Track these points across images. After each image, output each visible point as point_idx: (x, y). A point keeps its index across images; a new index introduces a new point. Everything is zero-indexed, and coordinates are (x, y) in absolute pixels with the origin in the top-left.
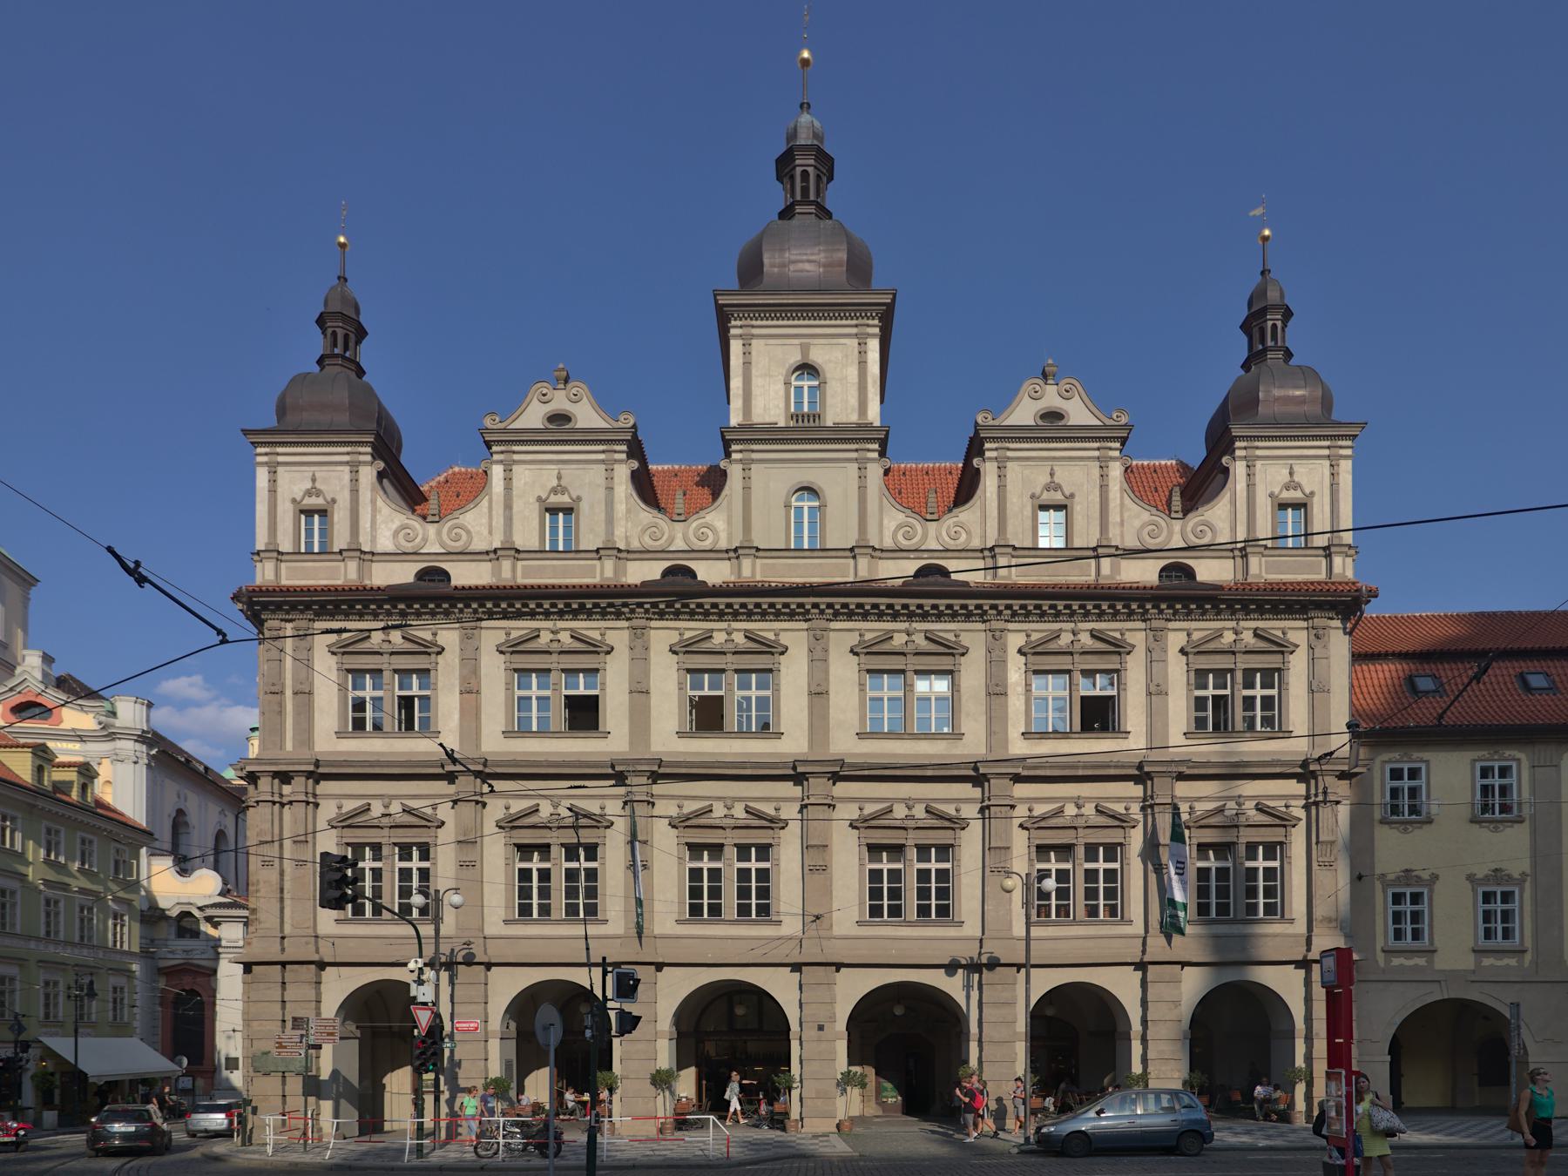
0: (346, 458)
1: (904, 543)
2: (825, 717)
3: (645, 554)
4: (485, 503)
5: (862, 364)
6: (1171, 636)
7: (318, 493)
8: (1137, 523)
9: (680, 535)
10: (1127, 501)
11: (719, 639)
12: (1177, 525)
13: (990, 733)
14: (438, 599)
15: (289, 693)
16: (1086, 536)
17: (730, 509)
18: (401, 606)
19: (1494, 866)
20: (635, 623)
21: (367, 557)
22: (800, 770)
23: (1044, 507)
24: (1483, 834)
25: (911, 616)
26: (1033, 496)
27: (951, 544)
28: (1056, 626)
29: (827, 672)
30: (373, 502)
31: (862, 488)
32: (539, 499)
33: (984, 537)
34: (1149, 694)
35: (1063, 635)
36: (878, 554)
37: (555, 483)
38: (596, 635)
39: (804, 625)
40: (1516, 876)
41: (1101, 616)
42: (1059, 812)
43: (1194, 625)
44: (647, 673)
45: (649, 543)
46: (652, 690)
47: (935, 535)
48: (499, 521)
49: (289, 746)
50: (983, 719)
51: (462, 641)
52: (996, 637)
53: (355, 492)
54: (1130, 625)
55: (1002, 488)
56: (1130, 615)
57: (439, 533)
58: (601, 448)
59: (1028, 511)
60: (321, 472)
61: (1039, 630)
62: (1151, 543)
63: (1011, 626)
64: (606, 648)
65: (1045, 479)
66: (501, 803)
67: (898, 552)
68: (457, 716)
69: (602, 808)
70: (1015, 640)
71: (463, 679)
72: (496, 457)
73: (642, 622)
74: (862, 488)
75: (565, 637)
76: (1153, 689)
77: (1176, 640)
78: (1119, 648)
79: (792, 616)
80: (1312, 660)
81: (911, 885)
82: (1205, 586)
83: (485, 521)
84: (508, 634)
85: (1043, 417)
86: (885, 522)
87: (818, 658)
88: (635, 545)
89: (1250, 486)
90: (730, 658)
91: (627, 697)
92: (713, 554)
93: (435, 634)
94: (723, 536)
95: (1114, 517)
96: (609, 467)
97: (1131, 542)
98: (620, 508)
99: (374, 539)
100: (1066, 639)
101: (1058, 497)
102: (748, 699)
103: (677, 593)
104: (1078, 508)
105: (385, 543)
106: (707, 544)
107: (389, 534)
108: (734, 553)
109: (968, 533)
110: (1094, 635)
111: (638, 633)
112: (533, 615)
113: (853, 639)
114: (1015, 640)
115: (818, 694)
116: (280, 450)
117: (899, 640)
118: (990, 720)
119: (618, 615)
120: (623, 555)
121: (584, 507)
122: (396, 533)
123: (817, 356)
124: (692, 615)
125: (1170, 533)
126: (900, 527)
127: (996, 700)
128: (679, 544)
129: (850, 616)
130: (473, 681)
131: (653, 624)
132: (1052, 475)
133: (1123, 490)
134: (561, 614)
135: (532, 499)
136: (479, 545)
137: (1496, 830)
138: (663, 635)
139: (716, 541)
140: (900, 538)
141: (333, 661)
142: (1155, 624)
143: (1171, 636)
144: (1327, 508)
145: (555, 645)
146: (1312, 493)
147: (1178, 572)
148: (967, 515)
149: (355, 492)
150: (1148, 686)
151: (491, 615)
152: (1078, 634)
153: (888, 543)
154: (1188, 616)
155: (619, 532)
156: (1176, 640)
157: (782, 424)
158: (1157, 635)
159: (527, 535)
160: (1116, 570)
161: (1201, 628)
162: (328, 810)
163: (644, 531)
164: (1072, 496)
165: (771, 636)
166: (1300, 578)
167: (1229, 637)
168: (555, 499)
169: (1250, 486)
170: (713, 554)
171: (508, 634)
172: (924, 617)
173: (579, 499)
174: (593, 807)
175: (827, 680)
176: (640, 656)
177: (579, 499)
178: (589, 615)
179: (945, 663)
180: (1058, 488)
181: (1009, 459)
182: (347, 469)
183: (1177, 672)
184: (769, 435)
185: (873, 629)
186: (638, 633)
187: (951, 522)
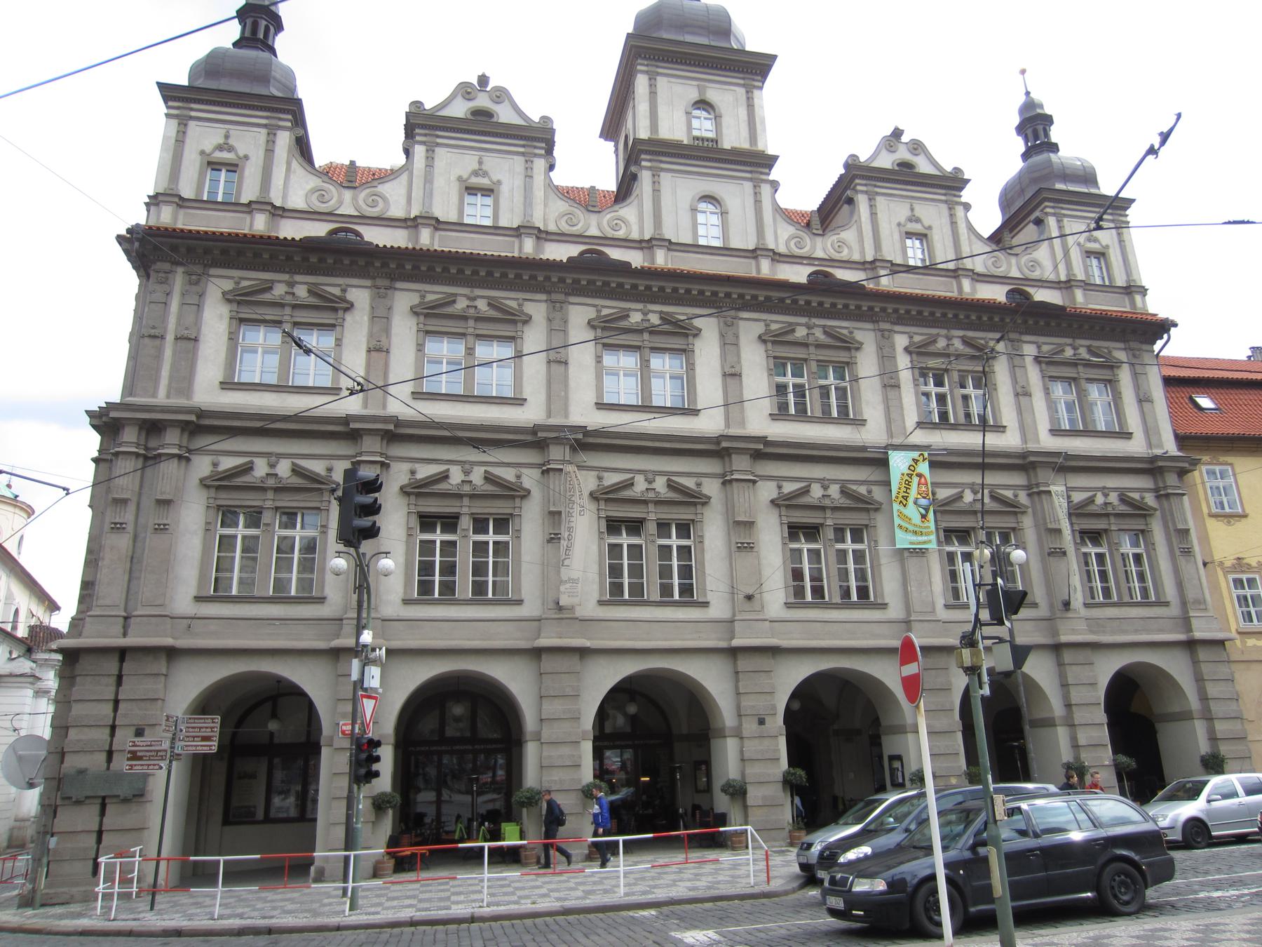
0: (264, 121)
1: (797, 252)
3: (561, 237)
7: (231, 149)
11: (636, 318)
12: (1013, 260)
13: (889, 420)
15: (170, 337)
17: (641, 206)
20: (555, 297)
23: (909, 235)
26: (899, 224)
27: (837, 256)
28: (934, 331)
29: (739, 356)
30: (289, 164)
32: (460, 179)
34: (1017, 395)
37: (476, 166)
43: (1041, 339)
45: (566, 228)
46: (570, 361)
47: (821, 247)
48: (417, 193)
51: (372, 299)
57: (355, 199)
58: (522, 142)
59: (896, 236)
60: (235, 131)
63: (897, 328)
64: (525, 318)
65: (907, 213)
66: (406, 467)
69: (518, 477)
70: (901, 341)
72: (418, 138)
73: (561, 297)
76: (1019, 390)
83: (403, 191)
84: (423, 297)
85: (899, 165)
86: (779, 232)
87: (729, 344)
88: (552, 227)
92: (626, 243)
93: (344, 291)
99: (285, 197)
100: (941, 343)
105: (297, 201)
106: (621, 234)
109: (850, 248)
110: (966, 341)
112: (452, 281)
114: (901, 341)
117: (801, 333)
120: (542, 235)
121: (505, 189)
122: (314, 191)
123: (713, 95)
125: (1010, 265)
127: (892, 393)
130: (383, 339)
132: (912, 210)
135: (453, 178)
136: (397, 211)
138: (580, 314)
140: (792, 244)
144: (1120, 258)
145: (472, 311)
148: (848, 235)
149: (270, 152)
150: (1014, 388)
152: (953, 340)
156: (1029, 350)
157: (685, 142)
159: (444, 209)
160: (974, 290)
168: (475, 181)
170: (626, 243)
171: (423, 297)
173: (499, 182)
174: (508, 474)
175: (739, 362)
177: (499, 182)
178: (510, 286)
180: (918, 220)
181: (877, 194)
182: (264, 131)
187: (835, 237)
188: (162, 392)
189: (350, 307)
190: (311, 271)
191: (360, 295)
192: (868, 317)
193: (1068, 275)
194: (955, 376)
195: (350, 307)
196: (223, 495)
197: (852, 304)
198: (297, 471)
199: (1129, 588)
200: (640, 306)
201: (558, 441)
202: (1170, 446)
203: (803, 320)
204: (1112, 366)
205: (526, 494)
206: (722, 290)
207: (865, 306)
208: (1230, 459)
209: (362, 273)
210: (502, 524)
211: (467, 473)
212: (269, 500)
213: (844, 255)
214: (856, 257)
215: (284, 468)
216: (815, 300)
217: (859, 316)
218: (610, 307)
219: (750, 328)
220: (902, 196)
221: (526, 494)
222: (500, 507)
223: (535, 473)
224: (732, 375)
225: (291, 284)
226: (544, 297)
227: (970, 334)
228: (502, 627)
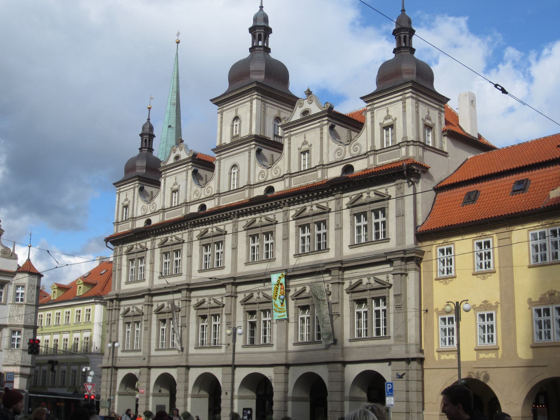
5: (251, 110)
9: (203, 193)
10: (330, 141)
19: (484, 299)
21: (134, 219)
22: (388, 257)
30: (138, 199)
31: (249, 160)
35: (307, 208)
36: (252, 186)
40: (494, 304)
42: (360, 283)
67: (259, 184)
74: (249, 160)
89: (373, 122)
96: (187, 171)
98: (189, 186)
100: (308, 211)
131: (194, 229)
133: (328, 138)
137: (484, 278)
142: (338, 196)
144: (402, 124)
146: (396, 119)
152: (311, 207)
162: (194, 302)
164: (311, 145)
166: (390, 161)
169: (373, 122)
172: (263, 210)
193: (371, 147)
199: (366, 327)
203: (258, 215)
208: (488, 233)
220: (301, 132)
228: (173, 358)
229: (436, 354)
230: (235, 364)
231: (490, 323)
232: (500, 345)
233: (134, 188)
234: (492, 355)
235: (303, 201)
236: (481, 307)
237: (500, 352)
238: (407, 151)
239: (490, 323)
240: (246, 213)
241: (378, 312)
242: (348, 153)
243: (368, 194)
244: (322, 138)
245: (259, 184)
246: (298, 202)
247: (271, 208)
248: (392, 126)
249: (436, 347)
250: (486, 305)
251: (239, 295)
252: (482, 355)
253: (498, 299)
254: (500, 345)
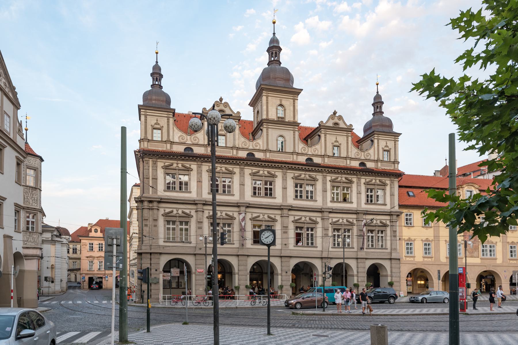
1: (304, 152)
2: (286, 194)
3: (243, 149)
4: (203, 131)
6: (362, 180)
8: (354, 152)
11: (261, 172)
12: (363, 153)
14: (189, 157)
15: (151, 178)
16: (344, 154)
18: (183, 158)
24: (424, 230)
25: (307, 171)
27: (314, 153)
28: (338, 175)
31: (294, 137)
33: (321, 152)
38: (231, 169)
39: (281, 171)
41: (348, 174)
43: (366, 177)
44: (201, 176)
47: (310, 151)
49: (151, 193)
50: (321, 197)
51: (197, 168)
52: (325, 177)
53: (168, 125)
54: (353, 176)
55: (325, 140)
56: (354, 174)
59: (331, 147)
61: (334, 176)
62: (357, 157)
63: (328, 175)
68: (196, 188)
70: (329, 178)
71: (198, 178)
74: (294, 137)
75: (223, 169)
77: (363, 181)
78: (351, 182)
79: (279, 168)
80: (391, 188)
81: (305, 235)
82: (368, 169)
87: (284, 179)
88: (240, 146)
90: (177, 171)
91: (239, 186)
92: (259, 150)
94: (262, 146)
95: (350, 150)
97: (353, 156)
100: (339, 179)
101: (337, 144)
102: (267, 188)
103: (250, 160)
104: (342, 147)
106: (258, 148)
107: (177, 137)
108: (264, 151)
110: (346, 178)
111: (242, 170)
113: (292, 175)
114: (329, 178)
115: (285, 188)
116: (147, 111)
117: (303, 176)
118: (323, 197)
119: (238, 164)
124: (256, 166)
125: (361, 155)
126: (303, 148)
128: (251, 147)
129: (293, 169)
134: (224, 163)
138: (248, 171)
139: (260, 147)
141: (162, 170)
142: (359, 177)
143: (362, 180)
147: (362, 164)
148: (318, 147)
151: (206, 162)
152: (342, 178)
153: (300, 152)
154: (366, 175)
155: (350, 154)
156: (363, 181)
158: (359, 179)
161: (368, 179)
163: (243, 143)
165: (273, 173)
166: (388, 168)
167: (374, 181)
170: (259, 150)
172: (310, 171)
176: (242, 175)
178: (231, 164)
179: (313, 183)
183: (363, 188)
184: (272, 122)
185: (297, 173)
186: (242, 170)
188: (151, 193)
189: (192, 170)
190: (183, 160)
191: (194, 166)
192: (321, 172)
194: (342, 188)
195: (192, 170)
196: (167, 218)
197: (317, 168)
198: (183, 212)
200: (262, 169)
201: (243, 206)
202: (397, 208)
204: (385, 185)
205: (235, 219)
206: (283, 165)
207: (320, 169)
209: (195, 161)
210: (229, 225)
211: (221, 213)
212: (178, 219)
213: (316, 153)
214: (319, 154)
215: (180, 212)
216: (307, 167)
217: (318, 171)
218: (255, 170)
219: (290, 174)
221: (235, 219)
222: (229, 221)
223: (237, 213)
224: (285, 188)
225: (177, 164)
226: (238, 167)
227: (347, 176)
229: (404, 258)
230: (267, 255)
231: (408, 246)
232: (433, 256)
233: (168, 118)
234: (430, 260)
235: (338, 173)
236: (407, 240)
237: (433, 259)
238: (395, 166)
239: (408, 246)
240: (298, 169)
241: (308, 234)
242: (363, 156)
243: (376, 180)
244: (347, 143)
245: (302, 154)
246: (335, 173)
247: (316, 171)
248: (388, 151)
249: (404, 255)
250: (427, 240)
251: (290, 217)
252: (426, 259)
253: (433, 238)
254: (433, 256)
